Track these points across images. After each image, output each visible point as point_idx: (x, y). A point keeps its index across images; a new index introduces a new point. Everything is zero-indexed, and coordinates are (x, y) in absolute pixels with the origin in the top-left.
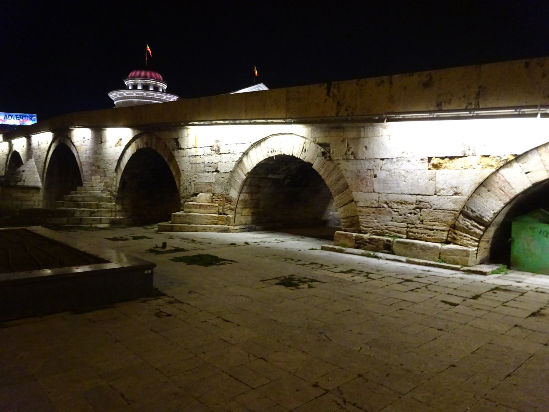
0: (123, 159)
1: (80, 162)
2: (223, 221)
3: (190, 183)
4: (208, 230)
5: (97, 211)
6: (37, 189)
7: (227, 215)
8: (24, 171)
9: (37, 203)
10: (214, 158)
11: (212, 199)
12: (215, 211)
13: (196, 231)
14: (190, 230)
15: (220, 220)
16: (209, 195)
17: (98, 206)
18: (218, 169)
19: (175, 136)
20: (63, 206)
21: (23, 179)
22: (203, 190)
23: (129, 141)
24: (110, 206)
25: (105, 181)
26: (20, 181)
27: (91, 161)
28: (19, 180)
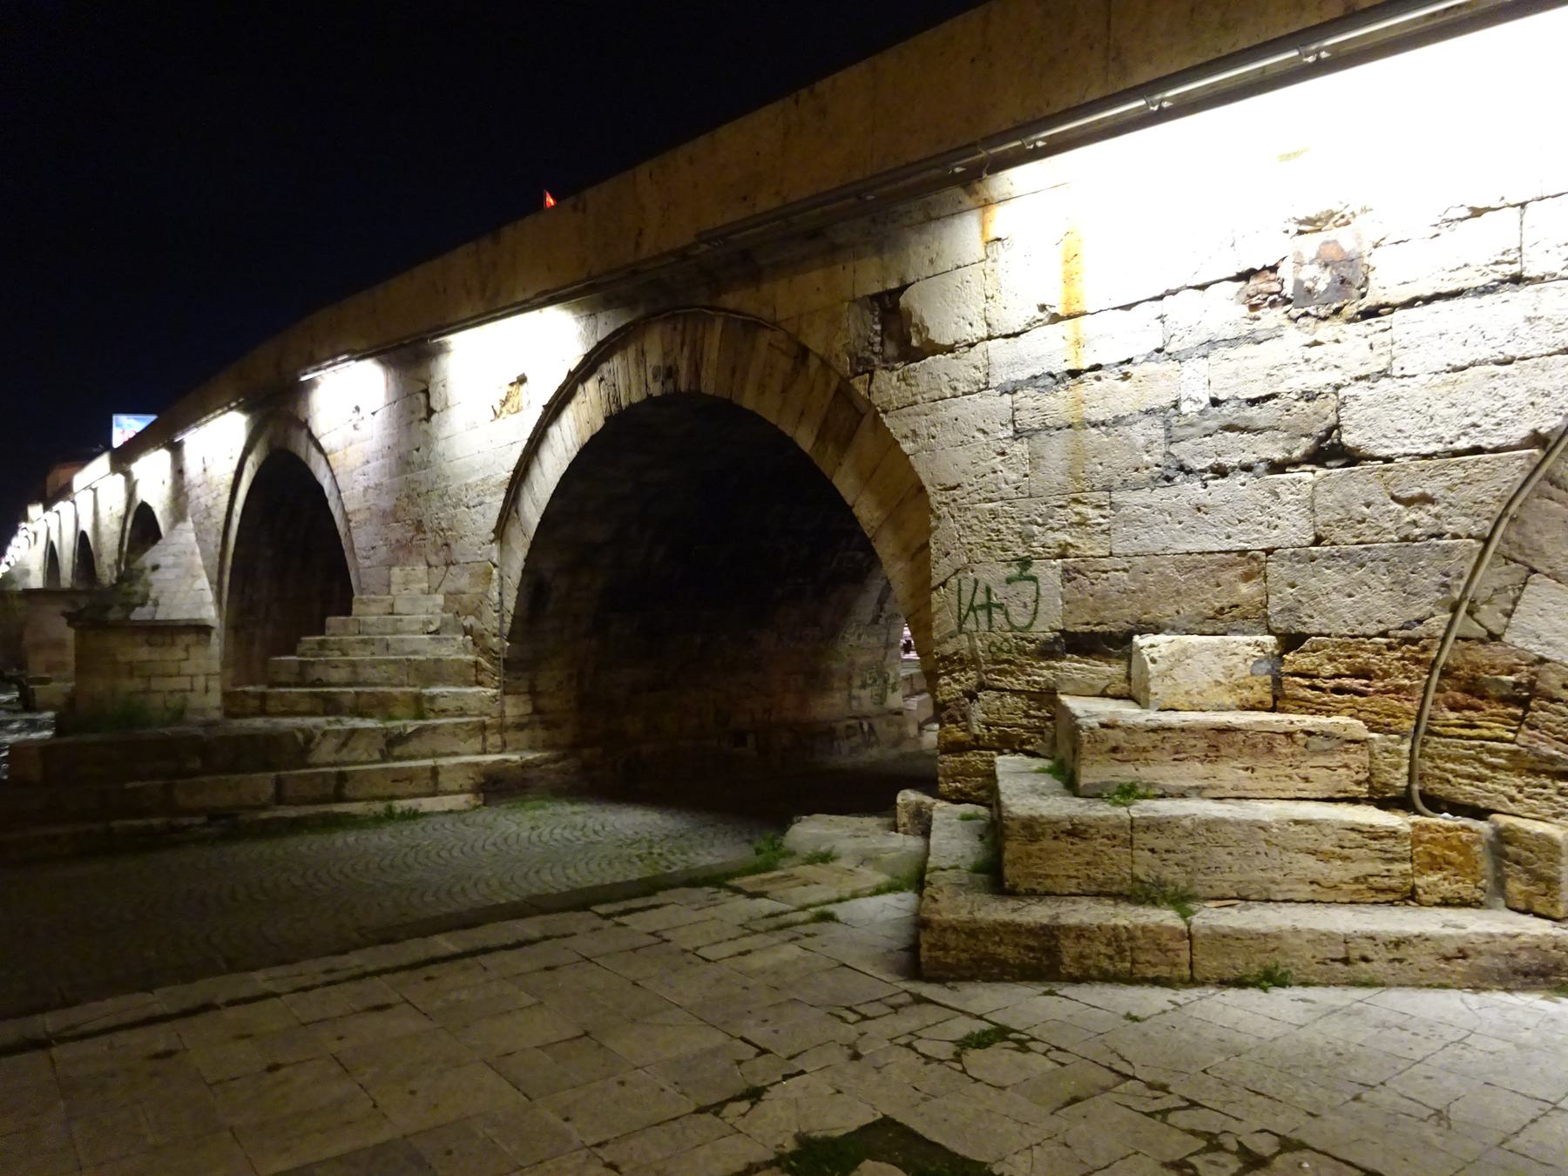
0: (536, 472)
1: (345, 513)
2: (1466, 868)
3: (1025, 563)
4: (1379, 967)
5: (419, 732)
6: (201, 629)
7: (1481, 814)
8: (155, 568)
9: (200, 683)
10: (1293, 361)
11: (1277, 682)
12: (1346, 780)
13: (1270, 979)
14: (1209, 965)
15: (1435, 864)
16: (1246, 649)
17: (420, 706)
18: (1349, 439)
19: (871, 278)
20: (262, 712)
21: (153, 595)
22: (1166, 612)
23: (563, 377)
24: (473, 703)
25: (449, 585)
26: (143, 605)
27: (386, 503)
28: (136, 599)
